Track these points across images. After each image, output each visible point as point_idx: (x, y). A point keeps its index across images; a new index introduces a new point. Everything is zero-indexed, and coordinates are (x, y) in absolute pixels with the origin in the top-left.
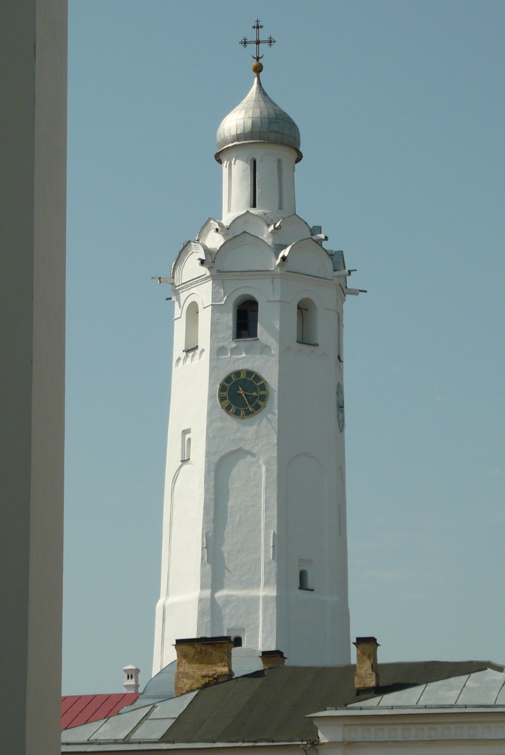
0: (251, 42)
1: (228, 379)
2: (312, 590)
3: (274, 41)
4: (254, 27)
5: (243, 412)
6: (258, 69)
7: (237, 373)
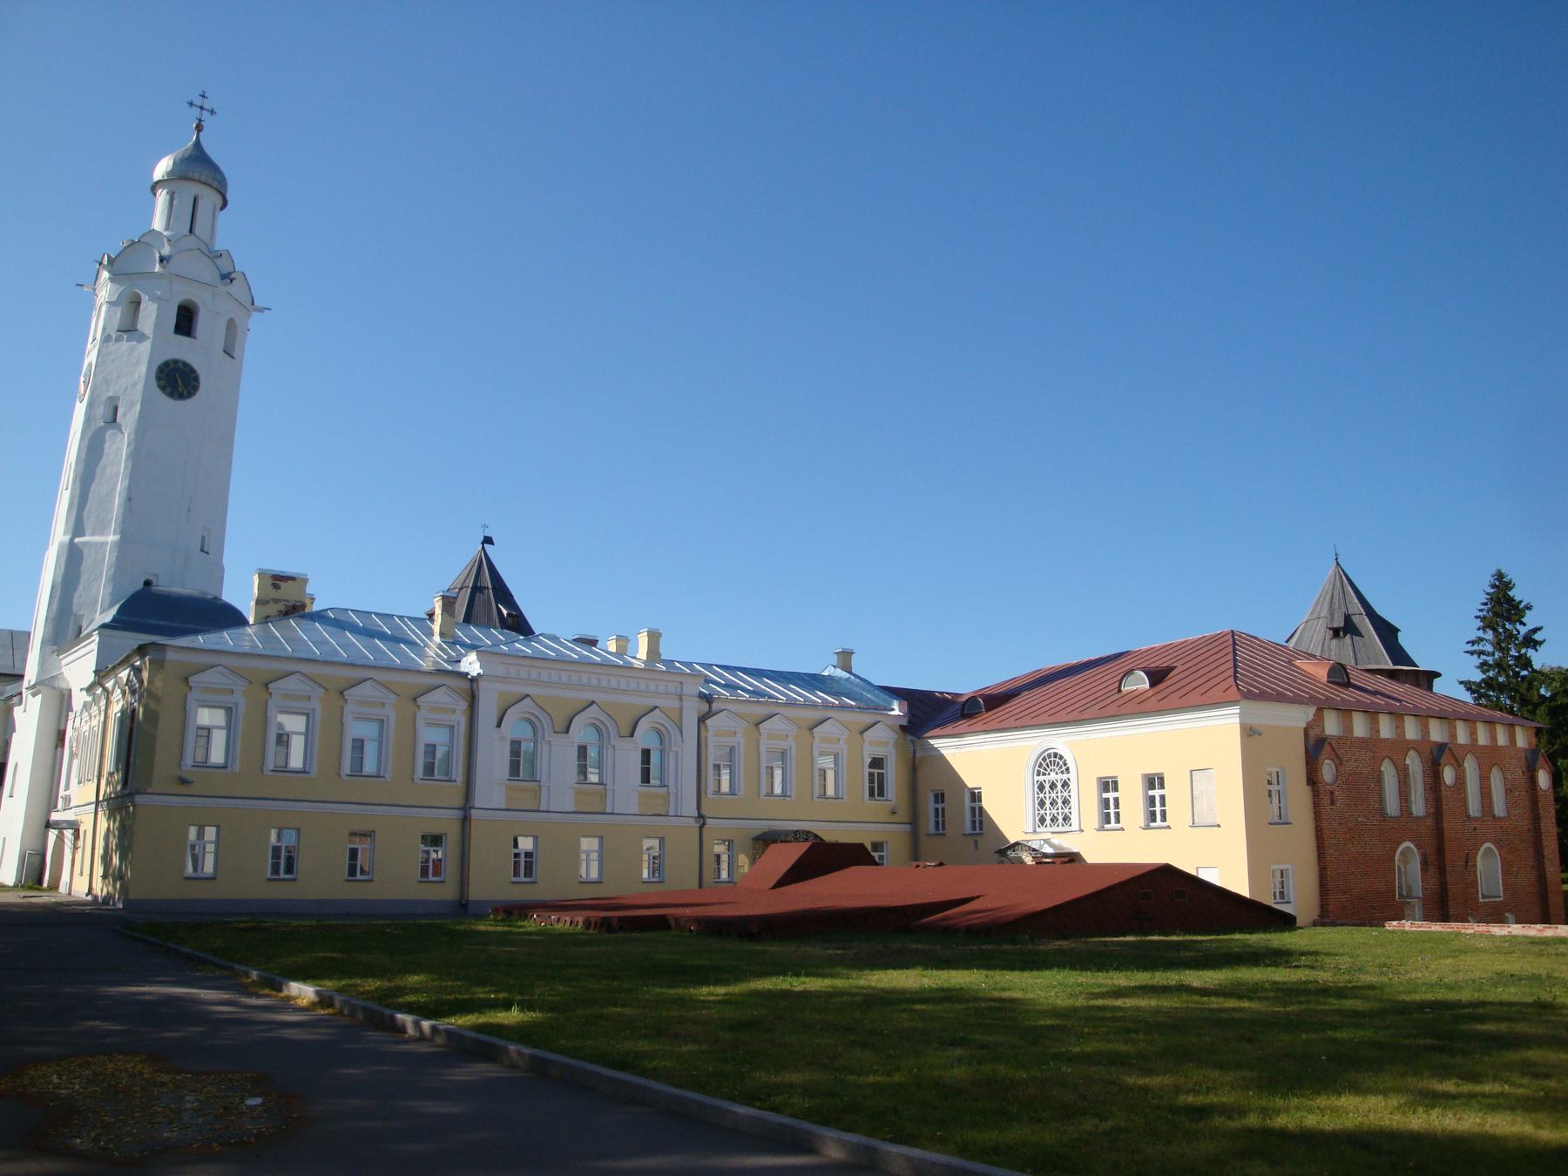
0: (196, 106)
1: (166, 364)
2: (207, 553)
4: (200, 95)
6: (199, 128)
7: (176, 362)
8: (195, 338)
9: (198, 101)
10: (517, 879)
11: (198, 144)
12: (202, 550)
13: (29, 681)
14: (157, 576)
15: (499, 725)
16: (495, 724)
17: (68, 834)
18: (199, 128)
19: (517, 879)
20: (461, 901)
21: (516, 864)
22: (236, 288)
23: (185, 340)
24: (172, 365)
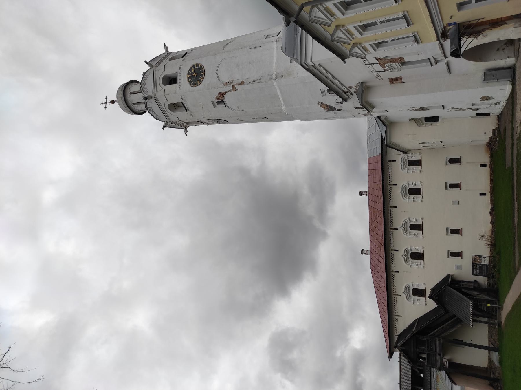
8: (177, 73)
9: (104, 105)
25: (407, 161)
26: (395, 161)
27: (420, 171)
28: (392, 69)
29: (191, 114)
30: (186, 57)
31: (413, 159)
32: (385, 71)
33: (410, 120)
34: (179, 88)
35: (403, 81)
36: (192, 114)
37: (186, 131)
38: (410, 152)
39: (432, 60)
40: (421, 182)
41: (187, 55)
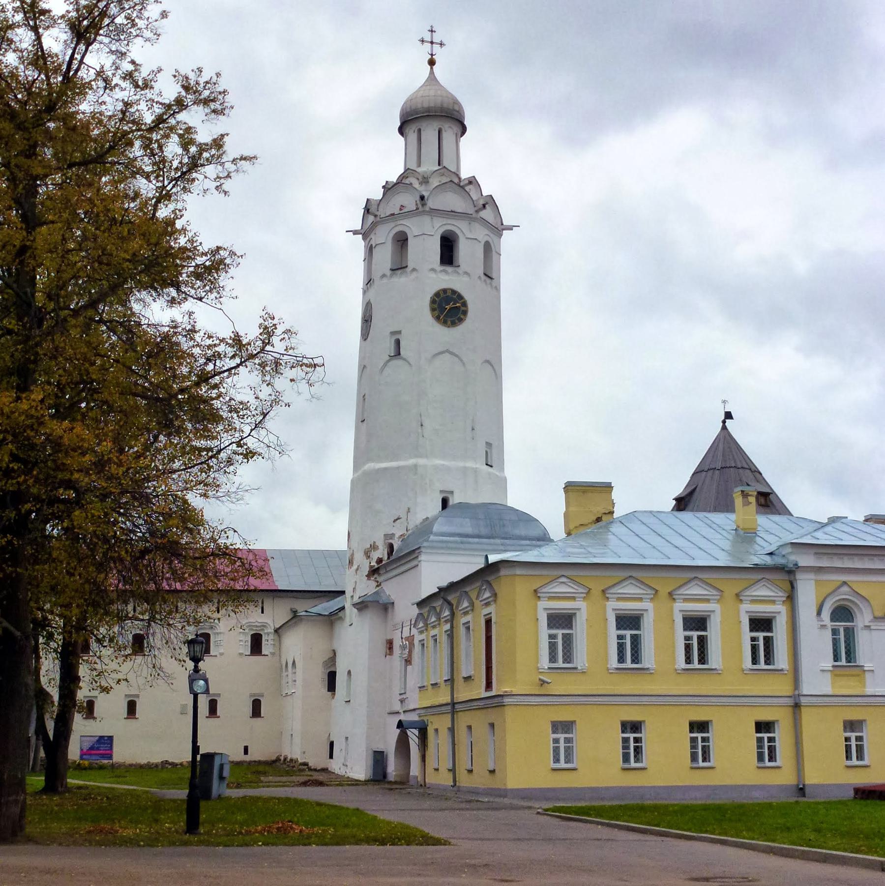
0: (427, 42)
2: (491, 466)
3: (444, 45)
5: (449, 323)
6: (432, 63)
7: (445, 291)
10: (849, 763)
11: (432, 77)
12: (487, 464)
13: (352, 597)
14: (452, 492)
15: (819, 613)
16: (815, 613)
17: (413, 735)
18: (432, 63)
19: (849, 763)
20: (798, 785)
21: (848, 749)
22: (487, 214)
23: (449, 269)
24: (442, 295)
25: (261, 633)
26: (262, 612)
27: (241, 654)
28: (403, 647)
29: (384, 276)
30: (485, 281)
31: (264, 642)
32: (402, 638)
33: (334, 652)
34: (433, 270)
35: (388, 656)
36: (385, 280)
37: (355, 232)
38: (276, 637)
39: (404, 696)
40: (222, 654)
41: (488, 280)
